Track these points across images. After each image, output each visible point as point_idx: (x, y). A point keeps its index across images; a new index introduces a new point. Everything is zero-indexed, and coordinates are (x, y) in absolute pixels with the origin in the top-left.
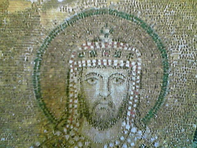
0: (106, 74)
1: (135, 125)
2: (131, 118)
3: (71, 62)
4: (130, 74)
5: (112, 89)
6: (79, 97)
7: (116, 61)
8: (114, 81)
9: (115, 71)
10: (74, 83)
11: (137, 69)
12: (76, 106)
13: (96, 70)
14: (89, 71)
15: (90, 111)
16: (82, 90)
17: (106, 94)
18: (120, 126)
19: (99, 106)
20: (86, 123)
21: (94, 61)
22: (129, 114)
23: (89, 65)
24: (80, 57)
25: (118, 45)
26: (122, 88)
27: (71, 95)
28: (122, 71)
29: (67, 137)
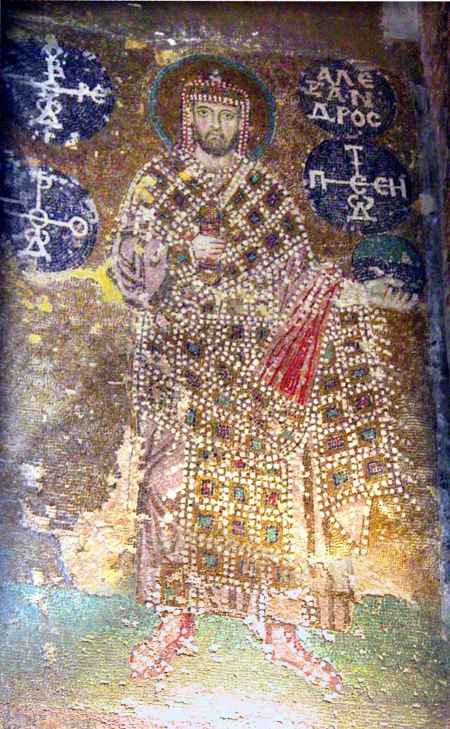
0: (217, 108)
1: (247, 157)
2: (242, 150)
3: (183, 94)
4: (239, 112)
5: (223, 123)
6: (192, 126)
7: (225, 99)
8: (224, 116)
9: (226, 108)
10: (187, 113)
11: (245, 109)
12: (189, 133)
13: (206, 104)
14: (200, 104)
15: (203, 140)
16: (195, 120)
17: (217, 126)
18: (232, 156)
19: (211, 137)
20: (199, 150)
21: (205, 96)
22: (240, 146)
23: (200, 99)
24: (190, 91)
25: (227, 86)
26: (232, 123)
27: (184, 123)
28: (231, 109)
29: (183, 158)
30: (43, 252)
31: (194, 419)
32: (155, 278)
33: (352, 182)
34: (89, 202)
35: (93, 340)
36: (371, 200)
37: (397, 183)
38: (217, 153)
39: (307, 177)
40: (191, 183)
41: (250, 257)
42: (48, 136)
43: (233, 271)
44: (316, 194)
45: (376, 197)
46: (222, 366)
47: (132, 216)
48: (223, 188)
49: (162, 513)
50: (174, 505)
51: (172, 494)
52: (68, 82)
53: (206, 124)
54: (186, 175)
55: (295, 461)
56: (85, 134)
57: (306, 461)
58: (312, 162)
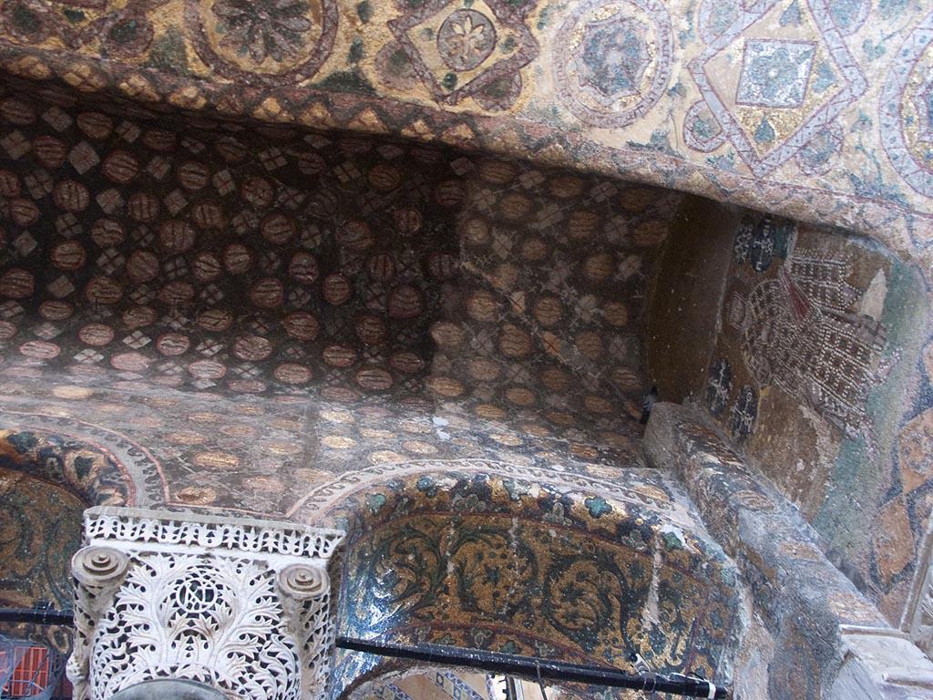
30: (750, 419)
31: (803, 369)
32: (767, 367)
33: (763, 247)
34: (746, 387)
35: (775, 408)
36: (769, 240)
37: (766, 224)
38: (745, 315)
39: (757, 271)
40: (750, 332)
41: (771, 313)
42: (728, 398)
43: (772, 323)
44: (763, 268)
45: (768, 237)
46: (793, 346)
47: (751, 368)
48: (753, 317)
49: (825, 402)
50: (823, 397)
51: (821, 394)
52: (718, 376)
53: (737, 318)
54: (747, 333)
55: (823, 319)
56: (729, 379)
57: (825, 313)
58: (754, 268)
